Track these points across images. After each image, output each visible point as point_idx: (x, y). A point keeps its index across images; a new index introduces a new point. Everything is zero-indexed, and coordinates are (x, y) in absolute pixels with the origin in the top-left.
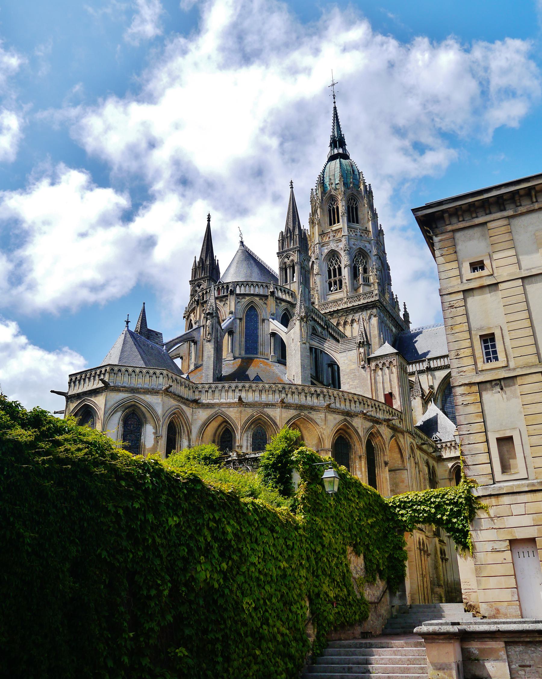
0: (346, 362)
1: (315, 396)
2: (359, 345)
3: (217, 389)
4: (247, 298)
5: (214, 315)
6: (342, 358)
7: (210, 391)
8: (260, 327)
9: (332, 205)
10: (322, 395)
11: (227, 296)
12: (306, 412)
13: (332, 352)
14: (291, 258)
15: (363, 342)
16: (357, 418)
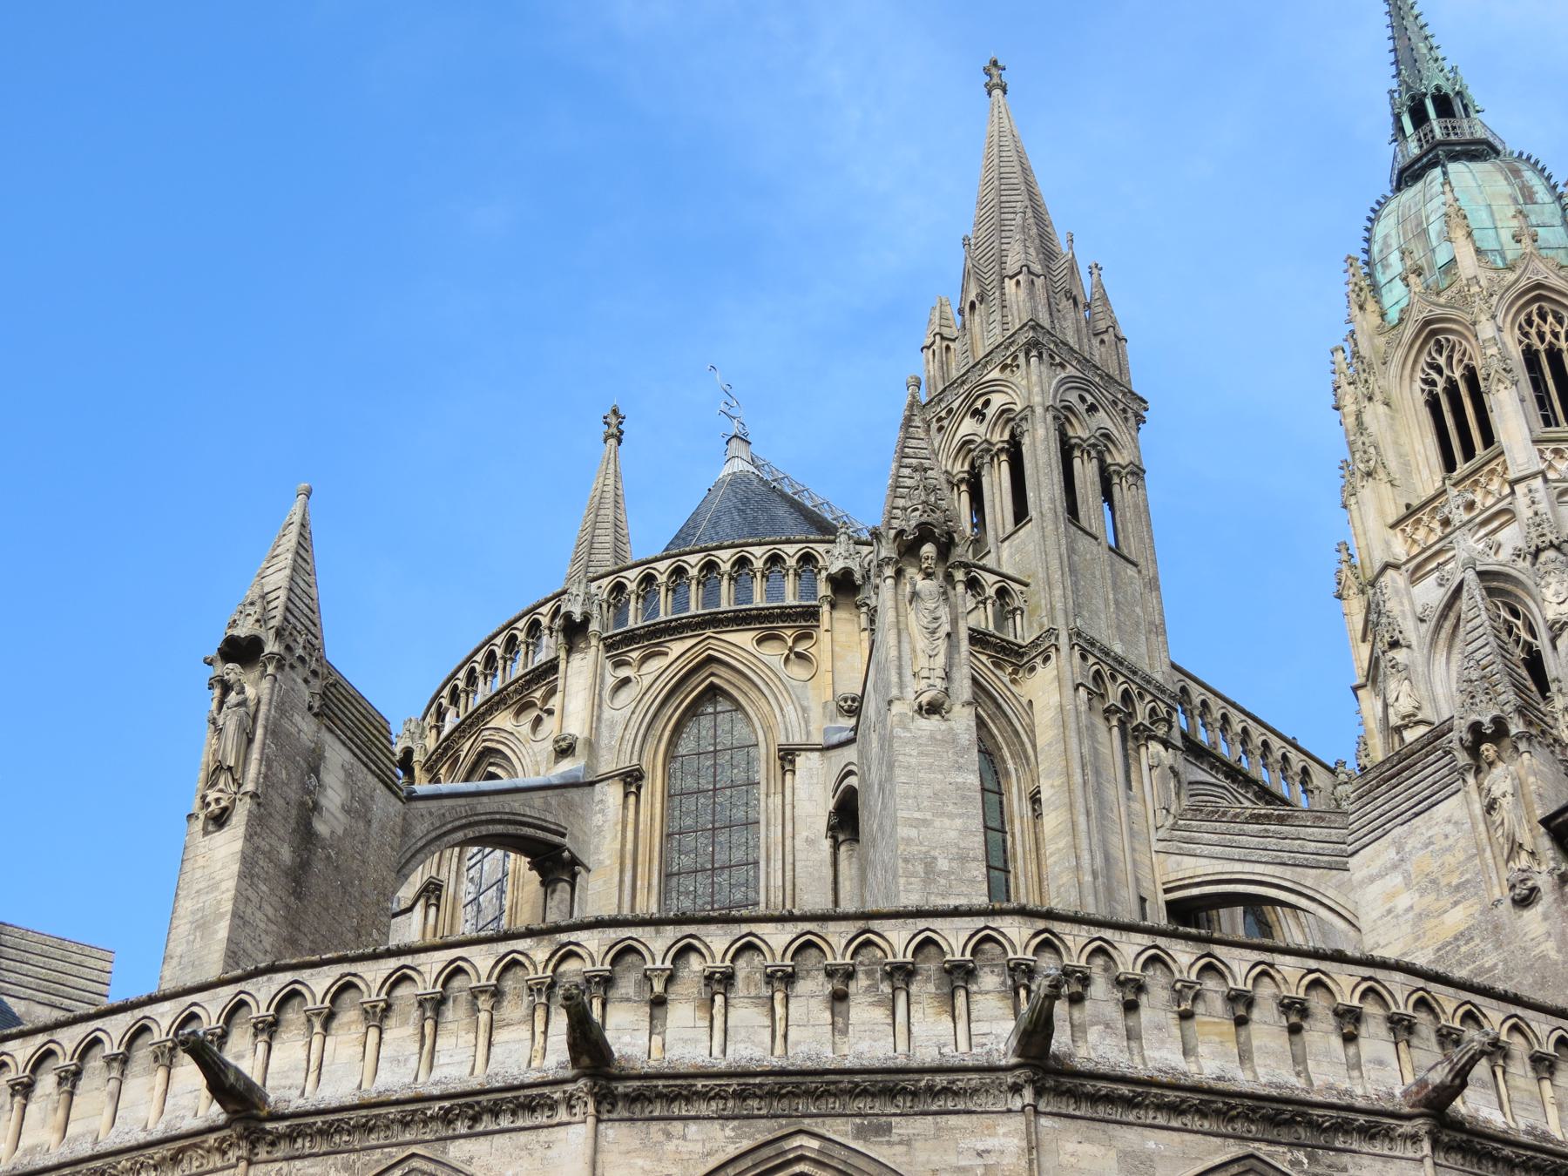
0: (1404, 901)
1: (924, 988)
2: (1474, 750)
3: (95, 1062)
4: (677, 648)
5: (271, 646)
6: (1375, 889)
7: (47, 1083)
8: (768, 805)
9: (1439, 371)
10: (989, 980)
11: (551, 667)
12: (840, 1130)
13: (1309, 878)
14: (997, 400)
15: (1499, 722)
16: (1380, 1147)
